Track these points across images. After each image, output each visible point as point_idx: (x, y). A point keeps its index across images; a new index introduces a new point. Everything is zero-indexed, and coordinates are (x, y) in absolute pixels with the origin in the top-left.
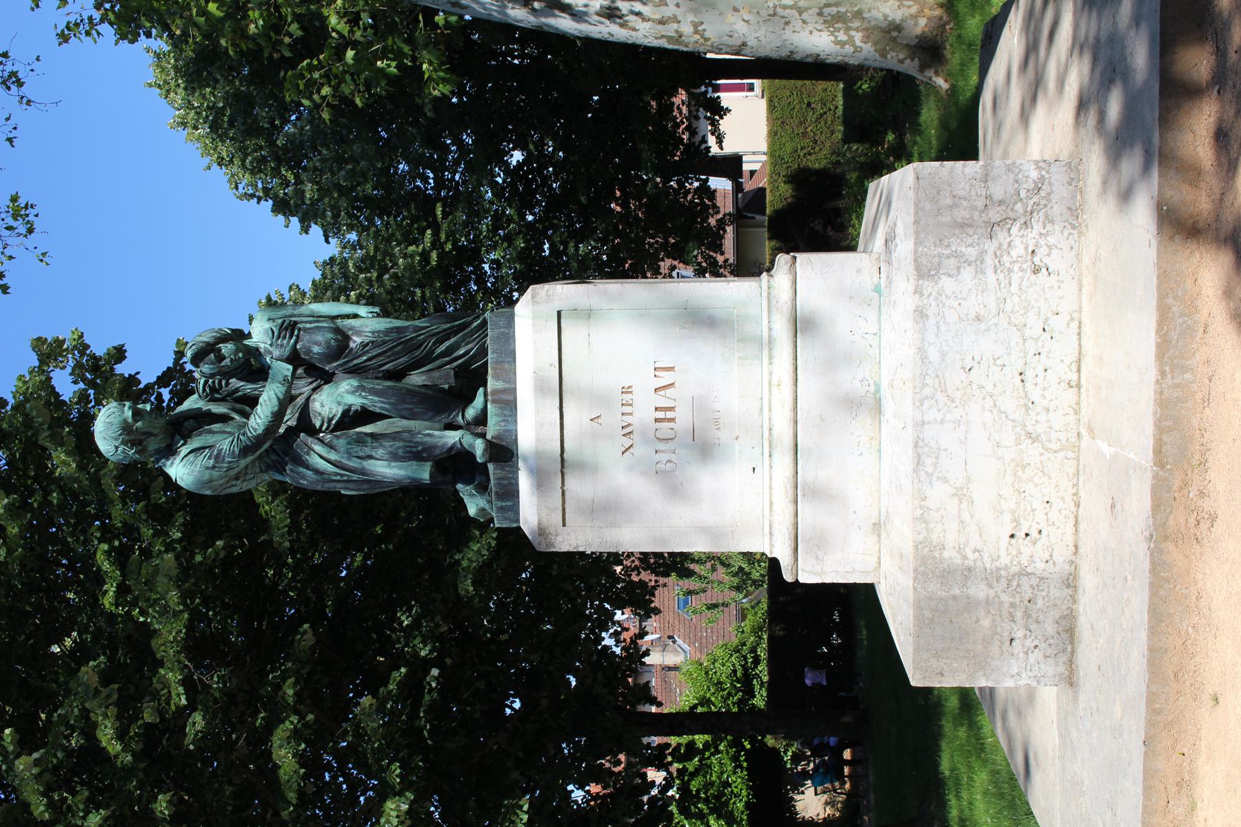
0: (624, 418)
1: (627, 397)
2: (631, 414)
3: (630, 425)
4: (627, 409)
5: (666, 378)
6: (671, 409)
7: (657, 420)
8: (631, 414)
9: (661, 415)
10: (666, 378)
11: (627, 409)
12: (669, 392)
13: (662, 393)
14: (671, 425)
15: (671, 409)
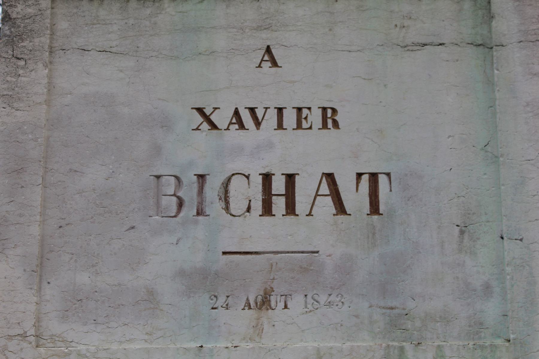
0: (272, 114)
1: (316, 117)
2: (280, 126)
3: (258, 123)
4: (290, 118)
5: (356, 198)
6: (291, 209)
7: (267, 178)
8: (280, 126)
9: (279, 185)
10: (356, 198)
11: (290, 118)
12: (326, 204)
13: (325, 189)
14: (258, 206)
15: (291, 208)
